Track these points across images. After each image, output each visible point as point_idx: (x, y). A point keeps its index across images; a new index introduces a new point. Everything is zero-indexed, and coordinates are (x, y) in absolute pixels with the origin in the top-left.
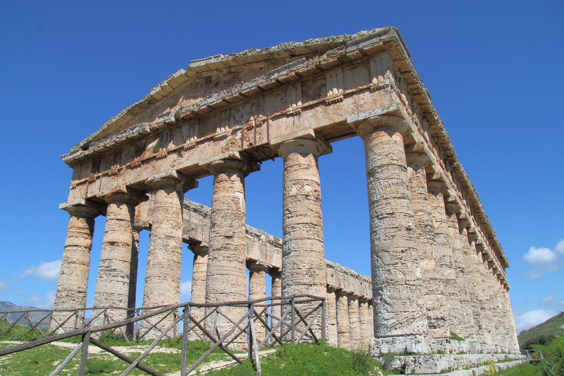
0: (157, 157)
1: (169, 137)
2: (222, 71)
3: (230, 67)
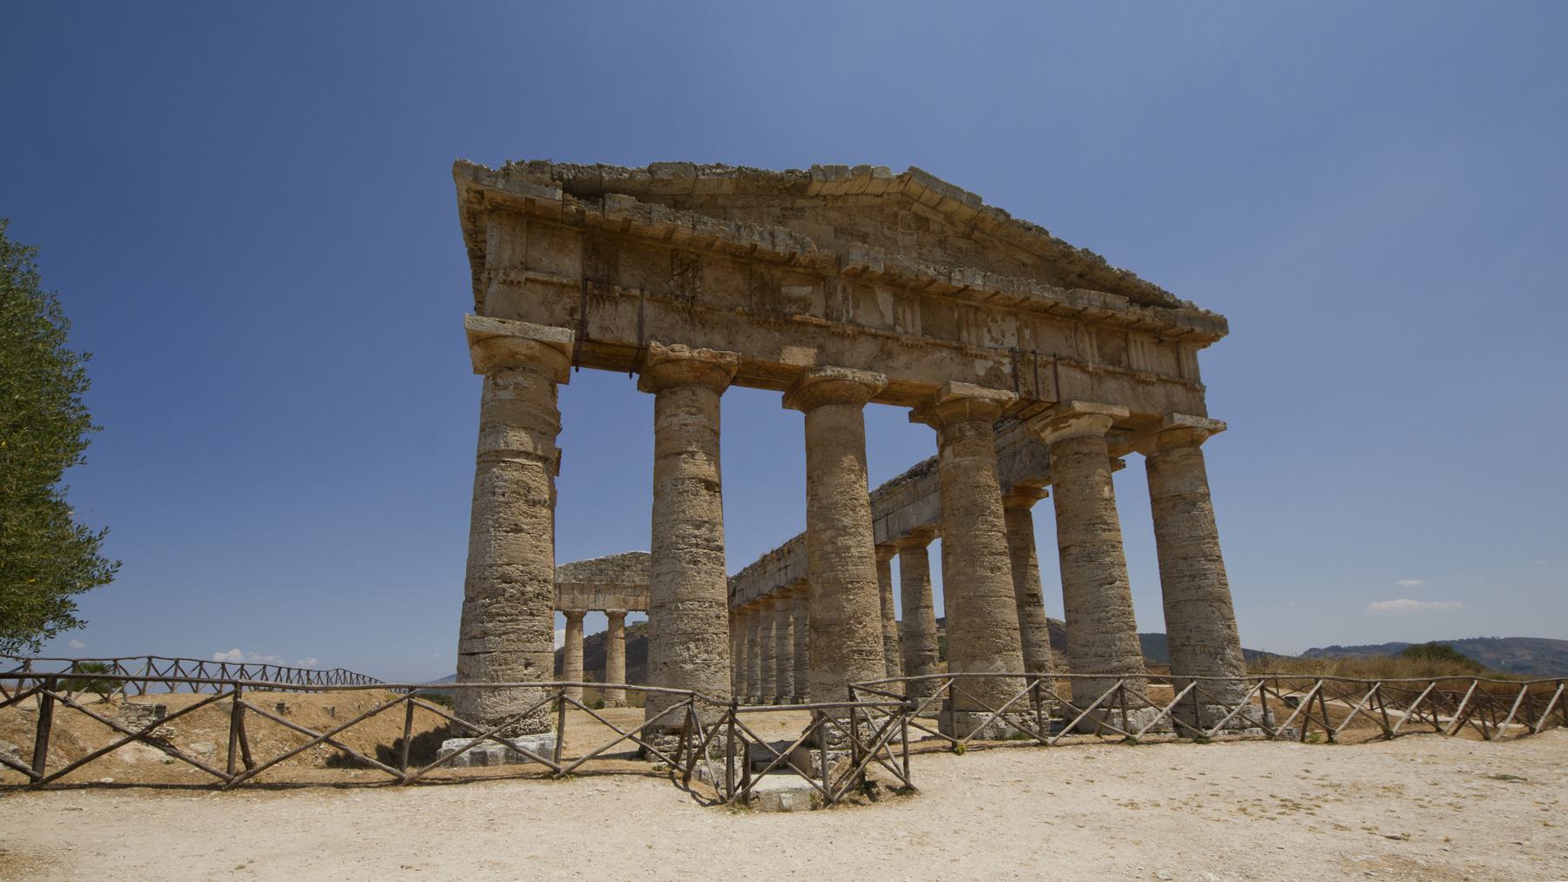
0: (831, 329)
1: (850, 298)
2: (953, 224)
3: (975, 227)
